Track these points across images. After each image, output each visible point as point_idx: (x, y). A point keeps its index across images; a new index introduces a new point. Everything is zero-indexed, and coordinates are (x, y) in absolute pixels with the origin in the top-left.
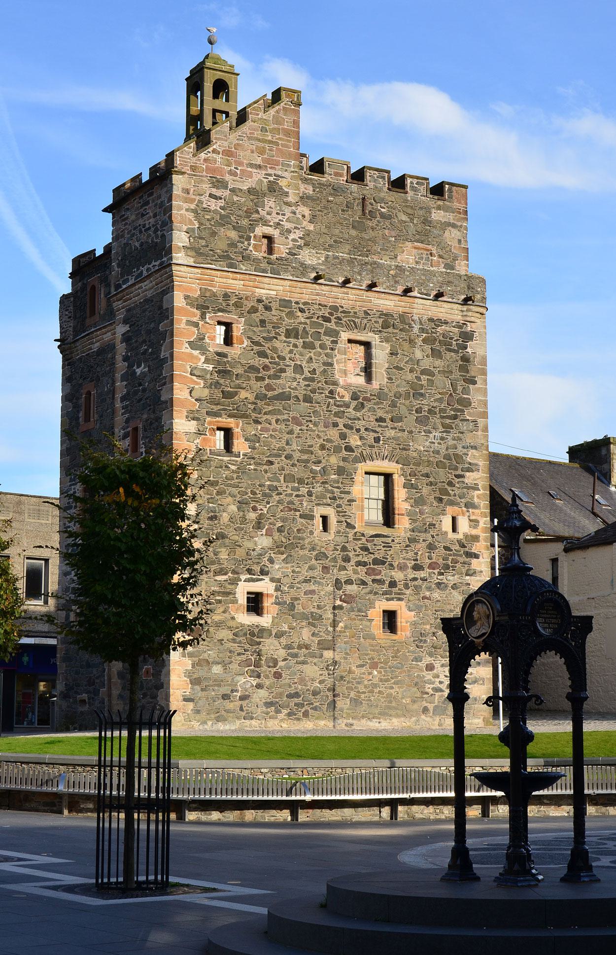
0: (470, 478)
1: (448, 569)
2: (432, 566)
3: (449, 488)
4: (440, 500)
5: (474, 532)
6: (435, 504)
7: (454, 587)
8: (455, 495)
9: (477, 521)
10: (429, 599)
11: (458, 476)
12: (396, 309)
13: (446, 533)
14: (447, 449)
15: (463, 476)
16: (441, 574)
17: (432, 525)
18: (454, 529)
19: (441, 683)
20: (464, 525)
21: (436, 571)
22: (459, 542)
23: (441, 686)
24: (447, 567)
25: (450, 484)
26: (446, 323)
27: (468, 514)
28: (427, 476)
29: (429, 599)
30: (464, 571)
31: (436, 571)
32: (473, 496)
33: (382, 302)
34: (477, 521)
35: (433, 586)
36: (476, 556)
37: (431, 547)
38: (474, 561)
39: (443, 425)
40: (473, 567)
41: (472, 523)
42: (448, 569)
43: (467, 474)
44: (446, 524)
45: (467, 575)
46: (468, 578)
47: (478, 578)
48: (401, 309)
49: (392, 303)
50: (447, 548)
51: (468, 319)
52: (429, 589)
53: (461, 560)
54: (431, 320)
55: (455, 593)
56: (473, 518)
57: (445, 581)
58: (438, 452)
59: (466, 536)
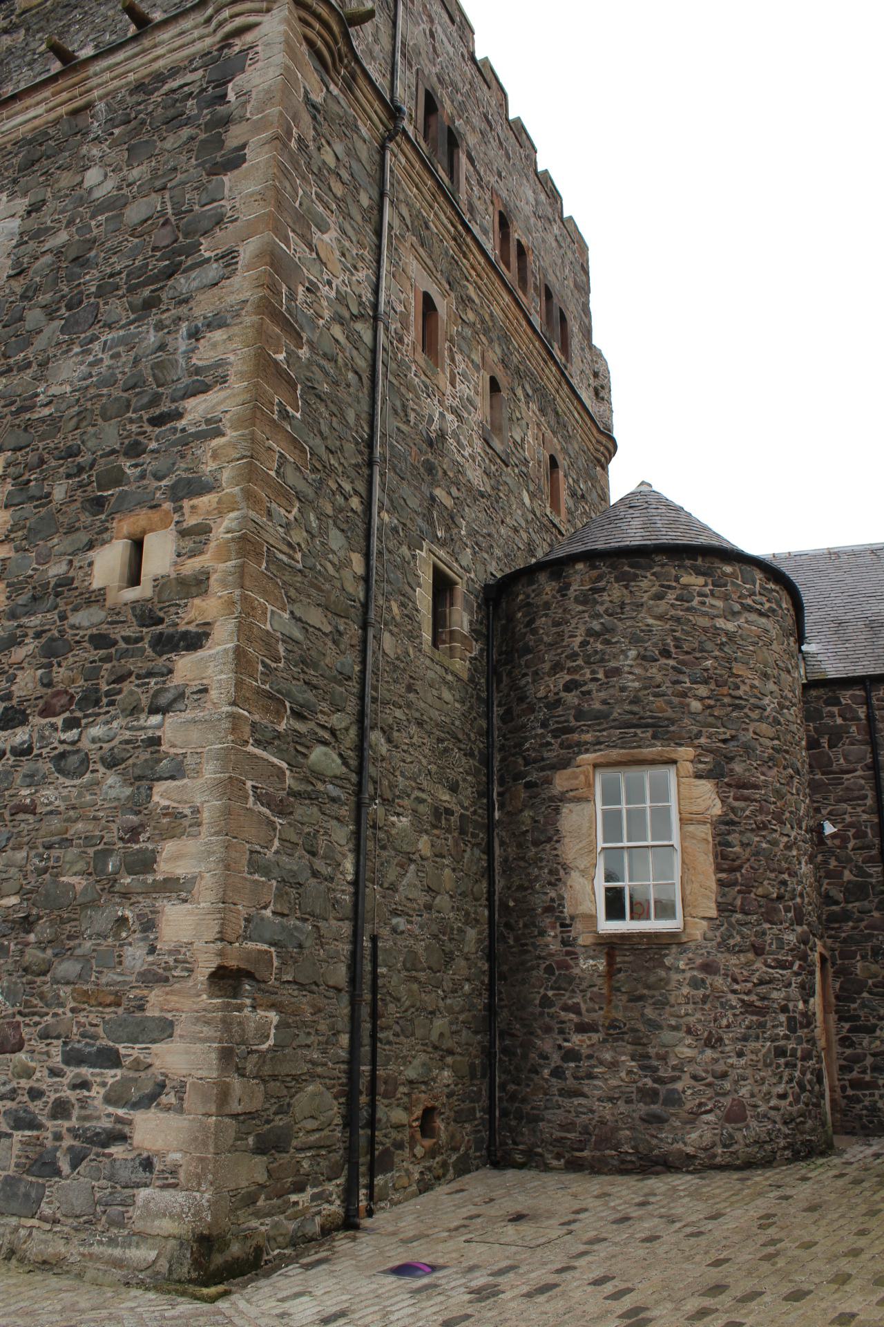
0: (196, 409)
1: (97, 703)
2: (46, 712)
3: (126, 464)
4: (98, 504)
5: (192, 566)
6: (86, 518)
7: (111, 763)
8: (142, 476)
9: (203, 530)
10: (31, 809)
11: (157, 421)
12: (53, 115)
13: (102, 591)
14: (136, 361)
15: (179, 415)
16: (70, 724)
17: (66, 582)
18: (134, 578)
19: (35, 1094)
20: (160, 556)
21: (59, 721)
22: (147, 615)
23: (36, 1107)
24: (91, 699)
25: (135, 450)
26: (174, 71)
27: (176, 517)
28: (72, 453)
29: (31, 809)
30: (145, 701)
31: (59, 721)
32: (198, 460)
33: (20, 119)
34: (203, 530)
35: (46, 766)
36: (194, 641)
37: (53, 650)
38: (186, 667)
39: (133, 308)
40: (177, 680)
41: (188, 544)
42: (97, 703)
43: (190, 403)
44: (107, 563)
45: (154, 710)
46: (155, 719)
47: (188, 715)
48: (63, 110)
49: (40, 110)
50: (101, 641)
51: (228, 28)
52: (32, 779)
53: (131, 664)
54: (139, 87)
55: (112, 779)
56: (191, 521)
57: (85, 744)
58: (110, 382)
59: (160, 583)
